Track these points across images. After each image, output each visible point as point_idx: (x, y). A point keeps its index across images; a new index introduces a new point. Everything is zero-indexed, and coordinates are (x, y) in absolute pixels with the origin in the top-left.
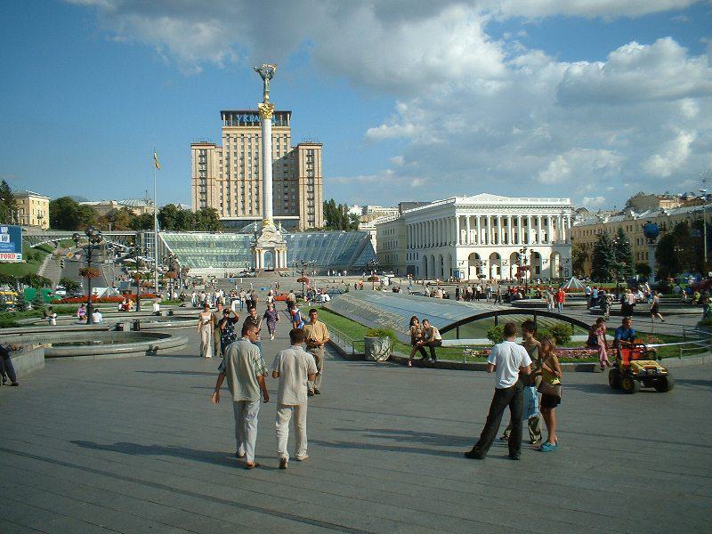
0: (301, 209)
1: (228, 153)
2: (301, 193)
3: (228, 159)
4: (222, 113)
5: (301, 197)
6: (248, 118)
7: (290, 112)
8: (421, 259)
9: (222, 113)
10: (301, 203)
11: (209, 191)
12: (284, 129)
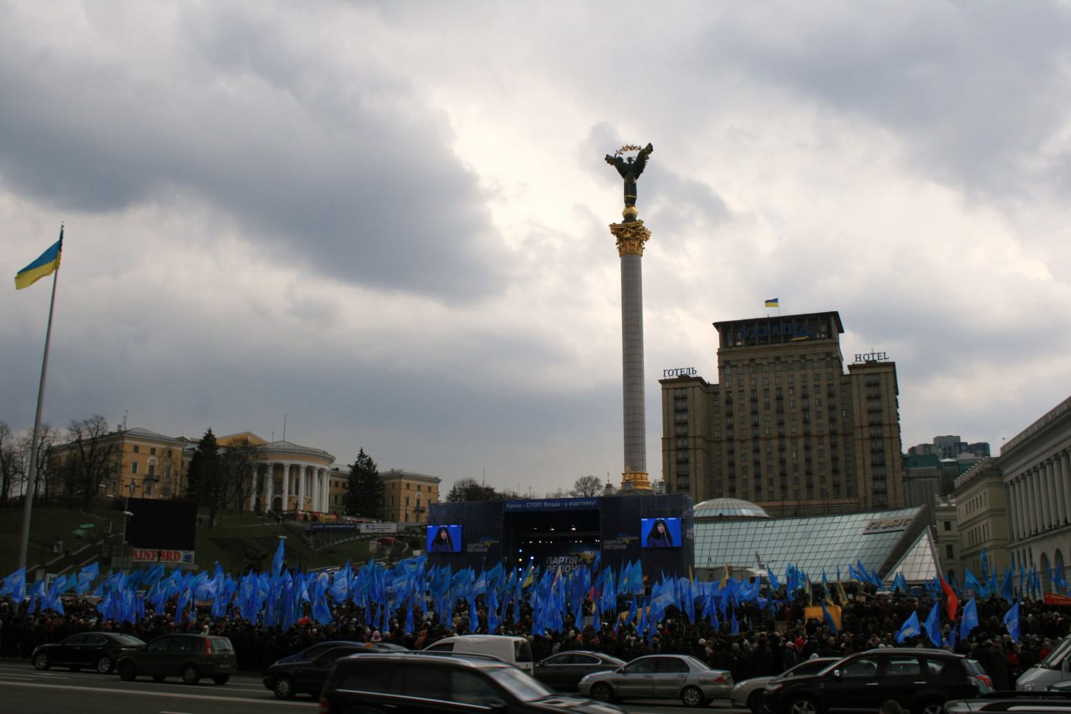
0: (861, 485)
1: (728, 393)
2: (859, 455)
3: (729, 402)
4: (717, 325)
5: (859, 462)
6: (761, 331)
8: (1037, 559)
9: (717, 325)
10: (860, 473)
11: (692, 459)
12: (825, 344)
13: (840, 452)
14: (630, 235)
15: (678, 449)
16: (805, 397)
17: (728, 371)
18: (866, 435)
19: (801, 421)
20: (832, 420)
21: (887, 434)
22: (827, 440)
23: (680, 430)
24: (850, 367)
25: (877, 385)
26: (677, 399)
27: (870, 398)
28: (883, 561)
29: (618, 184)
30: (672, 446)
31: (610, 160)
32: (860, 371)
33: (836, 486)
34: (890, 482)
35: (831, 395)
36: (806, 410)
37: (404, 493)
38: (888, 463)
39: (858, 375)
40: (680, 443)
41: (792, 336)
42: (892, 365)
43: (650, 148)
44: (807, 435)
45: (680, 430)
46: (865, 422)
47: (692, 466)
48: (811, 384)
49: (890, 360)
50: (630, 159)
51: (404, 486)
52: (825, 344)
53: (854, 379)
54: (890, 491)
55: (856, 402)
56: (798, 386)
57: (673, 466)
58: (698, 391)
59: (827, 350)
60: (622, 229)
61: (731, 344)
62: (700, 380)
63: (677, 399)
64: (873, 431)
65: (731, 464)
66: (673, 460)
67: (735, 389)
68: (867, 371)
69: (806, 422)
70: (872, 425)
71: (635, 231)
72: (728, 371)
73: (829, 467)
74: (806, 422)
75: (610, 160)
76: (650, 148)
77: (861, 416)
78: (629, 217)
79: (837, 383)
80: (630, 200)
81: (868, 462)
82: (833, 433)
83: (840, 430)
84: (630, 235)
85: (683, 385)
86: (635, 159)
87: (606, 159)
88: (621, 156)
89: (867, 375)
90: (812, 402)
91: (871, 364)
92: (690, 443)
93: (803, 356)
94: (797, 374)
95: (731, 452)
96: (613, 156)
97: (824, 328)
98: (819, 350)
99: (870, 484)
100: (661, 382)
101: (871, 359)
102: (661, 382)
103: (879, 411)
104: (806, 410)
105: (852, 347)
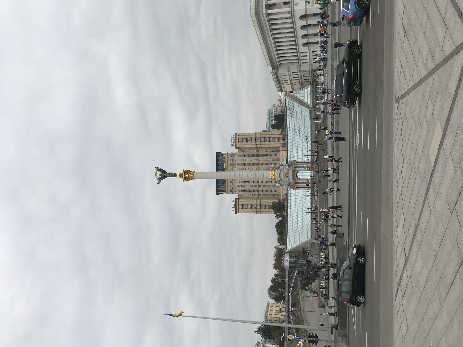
0: (276, 146)
2: (266, 146)
3: (245, 191)
4: (217, 194)
5: (268, 146)
7: (217, 153)
8: (306, 49)
9: (217, 194)
10: (272, 146)
11: (264, 203)
12: (227, 157)
13: (264, 153)
14: (187, 176)
15: (261, 208)
16: (245, 164)
17: (234, 190)
18: (259, 143)
19: (253, 166)
20: (253, 156)
21: (259, 136)
22: (260, 158)
23: (254, 207)
24: (236, 148)
25: (242, 139)
26: (242, 208)
27: (247, 141)
28: (303, 107)
29: (168, 178)
30: (259, 210)
31: (159, 183)
32: (237, 144)
33: (276, 155)
34: (275, 136)
35: (244, 156)
36: (249, 164)
37: (273, 316)
38: (269, 136)
40: (258, 207)
41: (223, 168)
42: (236, 134)
43: (157, 168)
44: (258, 164)
45: (254, 207)
46: (255, 143)
47: (266, 203)
48: (240, 162)
51: (270, 316)
52: (227, 157)
53: (239, 147)
54: (278, 136)
55: (248, 146)
56: (240, 167)
57: (266, 210)
58: (240, 200)
59: (229, 156)
61: (224, 190)
62: (236, 199)
63: (242, 208)
64: (258, 140)
65: (267, 191)
66: (264, 210)
67: (241, 188)
68: (237, 142)
69: (253, 164)
70: (256, 141)
72: (234, 190)
73: (270, 157)
74: (253, 164)
75: (159, 183)
76: (157, 168)
77: (252, 145)
78: (181, 176)
79: (240, 154)
80: (175, 175)
81: (268, 143)
82: (258, 156)
83: (257, 153)
84: (187, 176)
85: (238, 205)
86: (160, 173)
90: (246, 162)
91: (235, 141)
92: (258, 203)
93: (231, 165)
94: (237, 167)
95: (262, 191)
97: (221, 157)
98: (229, 159)
99: (276, 143)
100: (236, 213)
102: (236, 213)
103: (251, 138)
104: (249, 164)
105: (228, 148)
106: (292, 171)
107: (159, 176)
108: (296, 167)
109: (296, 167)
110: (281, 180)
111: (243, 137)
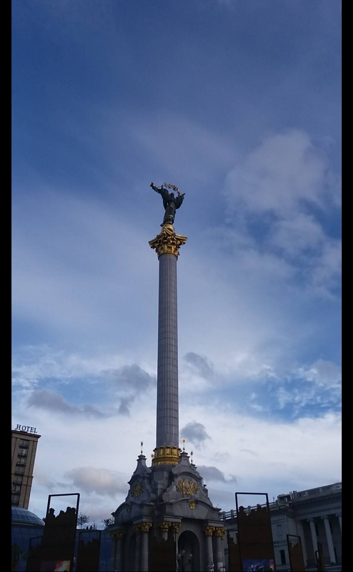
21: (25, 483)
32: (18, 436)
39: (16, 438)
49: (37, 434)
50: (172, 195)
60: (170, 236)
68: (23, 437)
71: (179, 242)
87: (152, 185)
88: (167, 189)
89: (21, 439)
96: (158, 186)
101: (26, 431)
103: (24, 466)
106: (203, 517)
107: (170, 191)
108: (215, 532)
109: (215, 532)
110: (172, 477)
111: (30, 450)
